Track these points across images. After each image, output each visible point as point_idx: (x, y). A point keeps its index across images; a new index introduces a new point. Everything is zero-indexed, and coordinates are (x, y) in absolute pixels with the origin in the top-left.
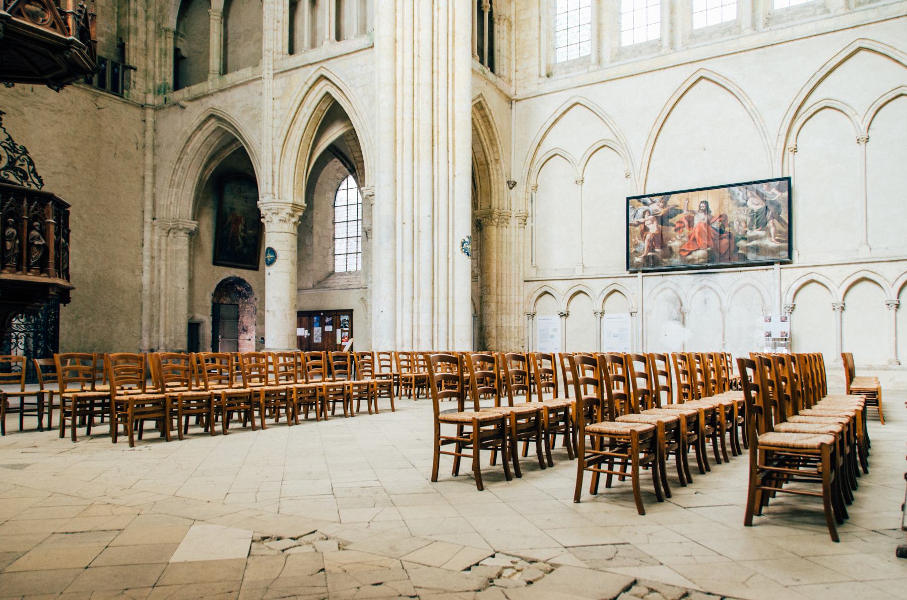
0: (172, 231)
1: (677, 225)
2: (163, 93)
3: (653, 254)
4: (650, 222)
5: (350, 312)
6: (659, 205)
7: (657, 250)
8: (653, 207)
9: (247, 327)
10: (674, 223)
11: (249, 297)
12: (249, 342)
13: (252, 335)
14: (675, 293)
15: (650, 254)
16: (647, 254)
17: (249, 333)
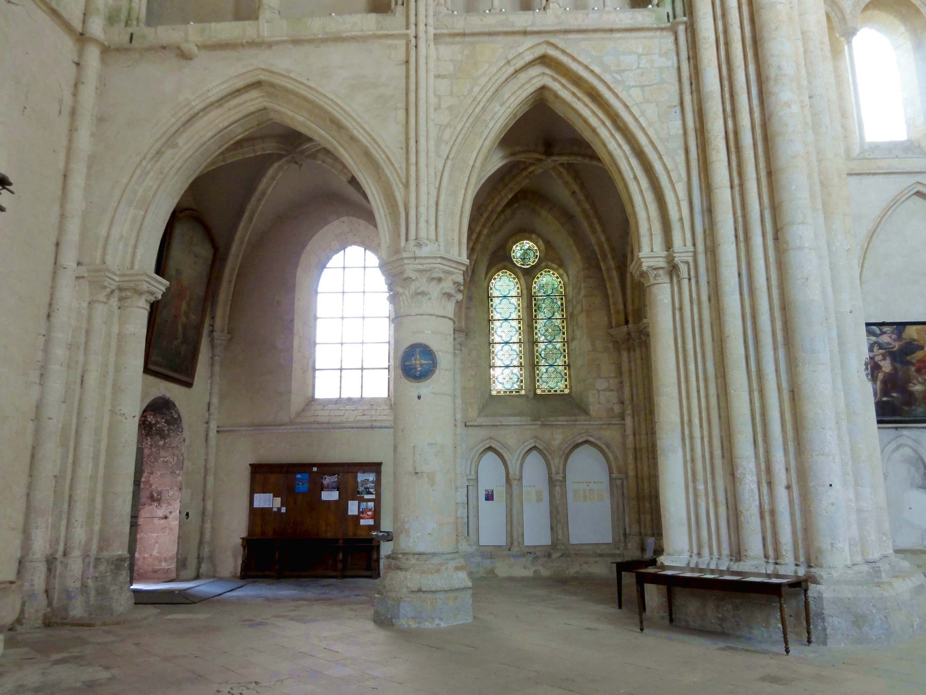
0: (117, 293)
1: (917, 365)
2: (122, 25)
3: (889, 399)
4: (880, 357)
5: (376, 467)
6: (890, 337)
7: (894, 395)
8: (885, 339)
9: (160, 493)
10: (914, 361)
11: (168, 435)
12: (162, 521)
13: (170, 508)
14: (916, 451)
15: (884, 399)
16: (881, 398)
17: (164, 505)
